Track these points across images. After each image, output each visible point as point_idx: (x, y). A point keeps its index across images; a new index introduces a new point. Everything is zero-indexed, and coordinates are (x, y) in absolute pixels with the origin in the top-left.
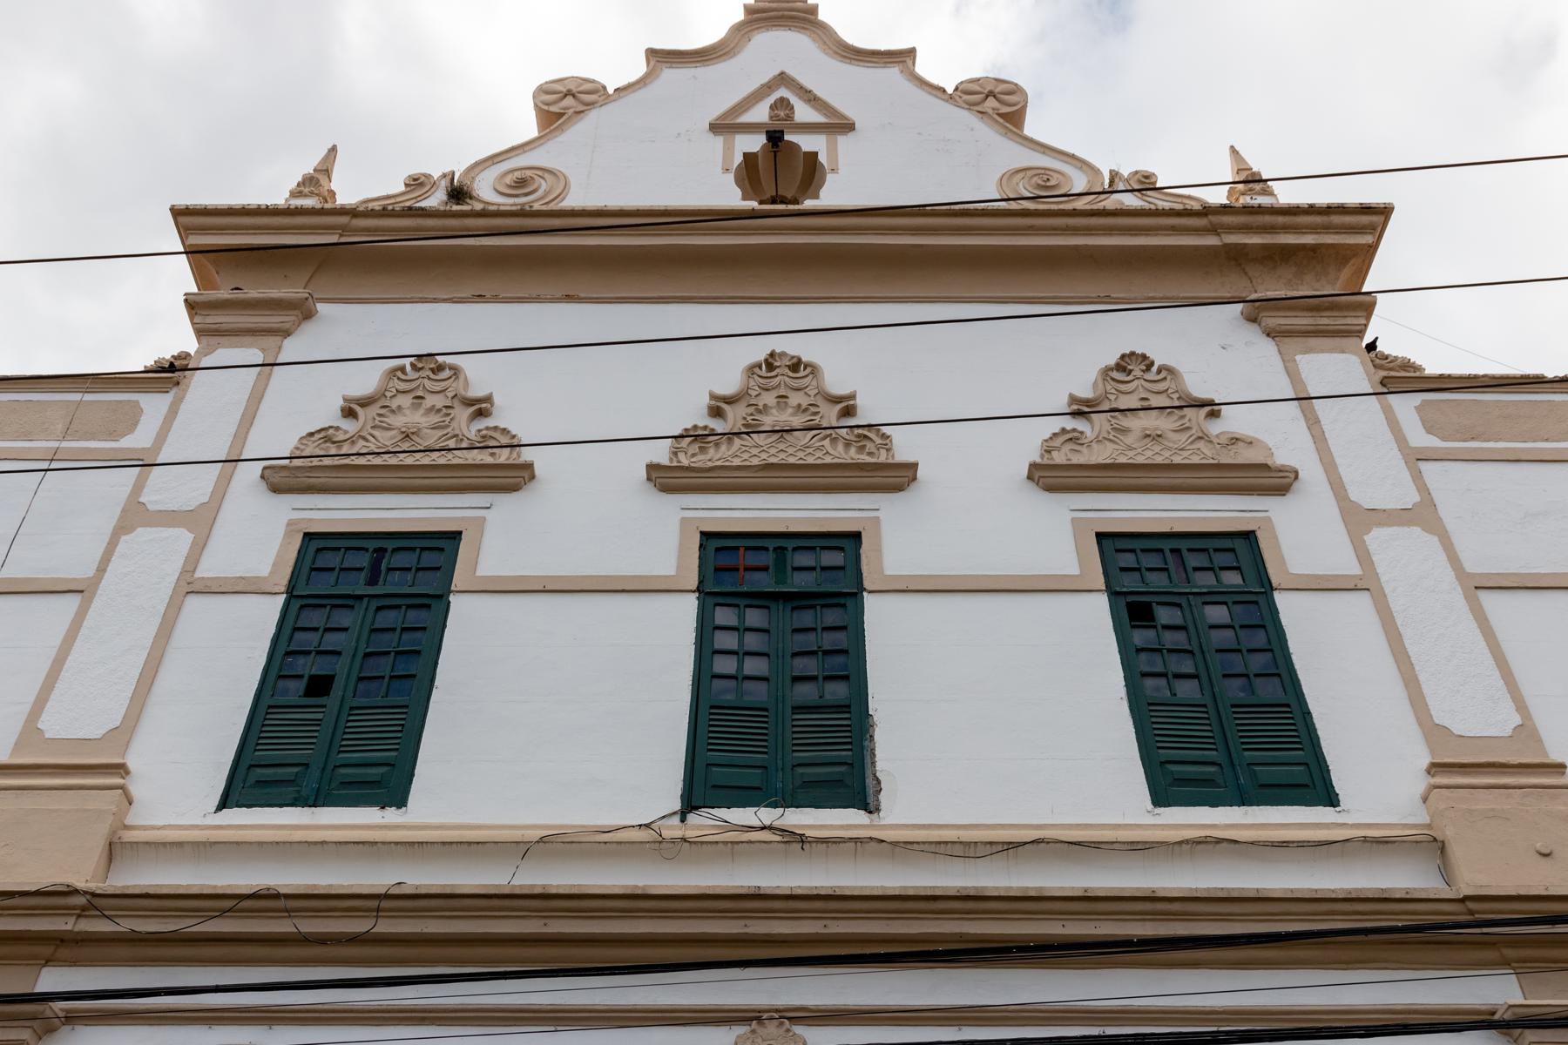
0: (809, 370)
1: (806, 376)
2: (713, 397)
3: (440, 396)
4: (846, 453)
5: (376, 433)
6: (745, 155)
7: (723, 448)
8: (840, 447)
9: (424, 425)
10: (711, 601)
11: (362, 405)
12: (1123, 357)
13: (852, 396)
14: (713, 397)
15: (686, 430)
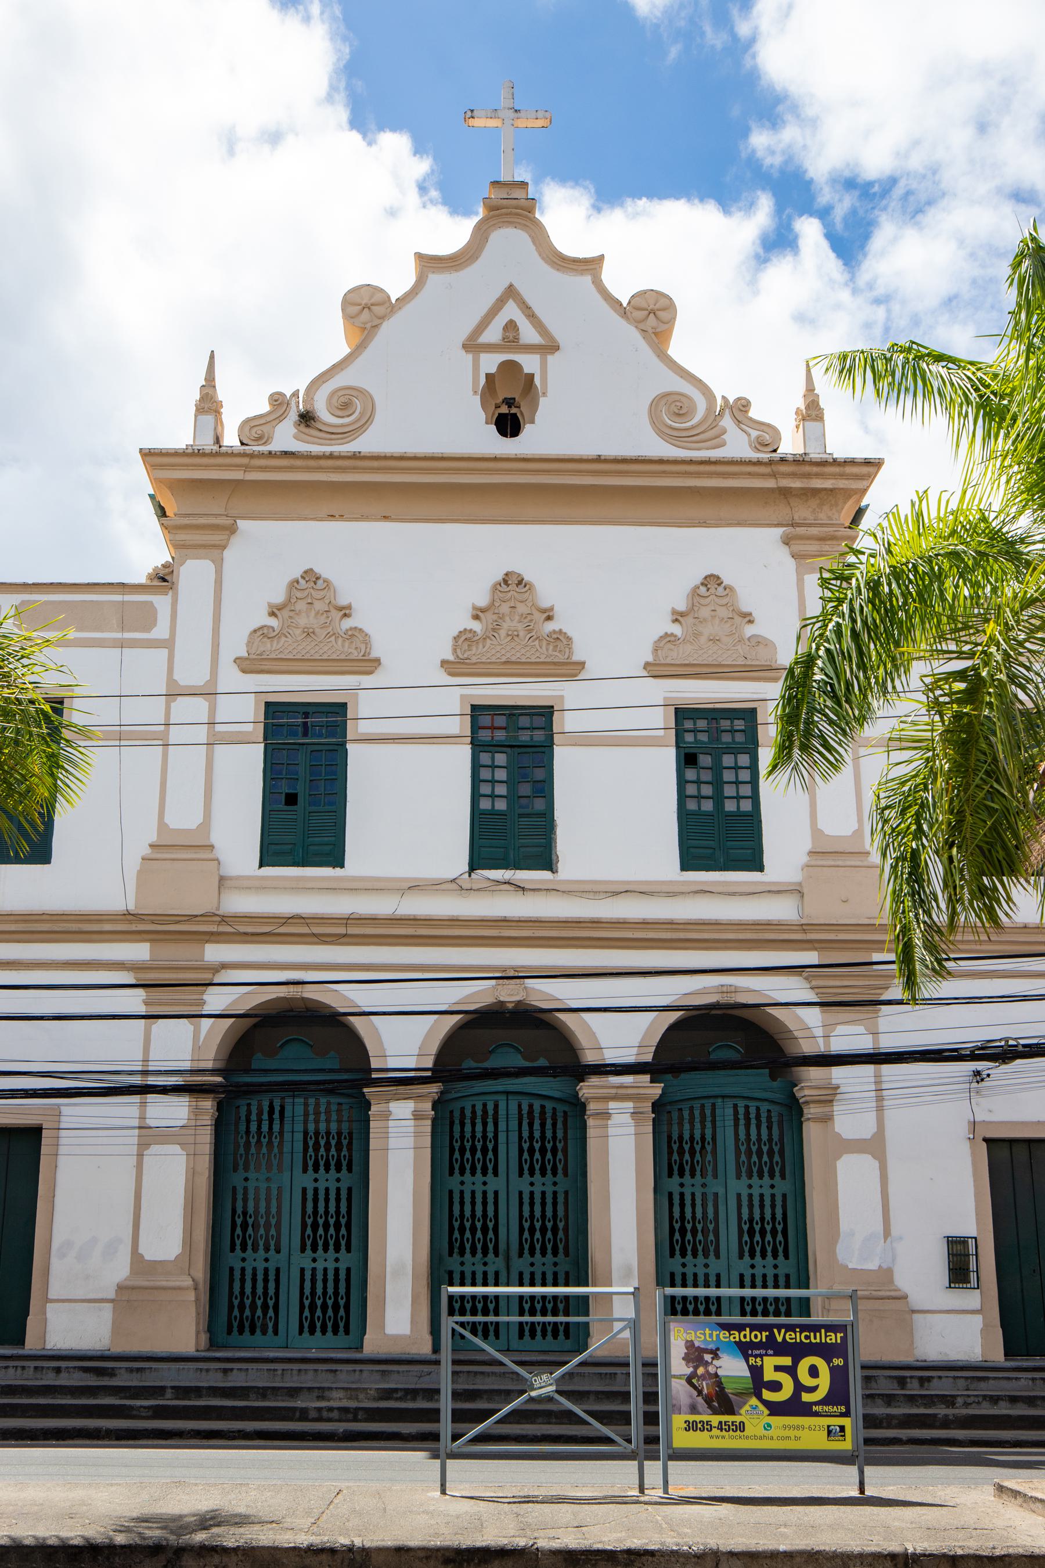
2: (475, 608)
7: (481, 646)
10: (478, 749)
11: (279, 610)
12: (706, 578)
13: (552, 609)
14: (475, 608)
15: (460, 632)
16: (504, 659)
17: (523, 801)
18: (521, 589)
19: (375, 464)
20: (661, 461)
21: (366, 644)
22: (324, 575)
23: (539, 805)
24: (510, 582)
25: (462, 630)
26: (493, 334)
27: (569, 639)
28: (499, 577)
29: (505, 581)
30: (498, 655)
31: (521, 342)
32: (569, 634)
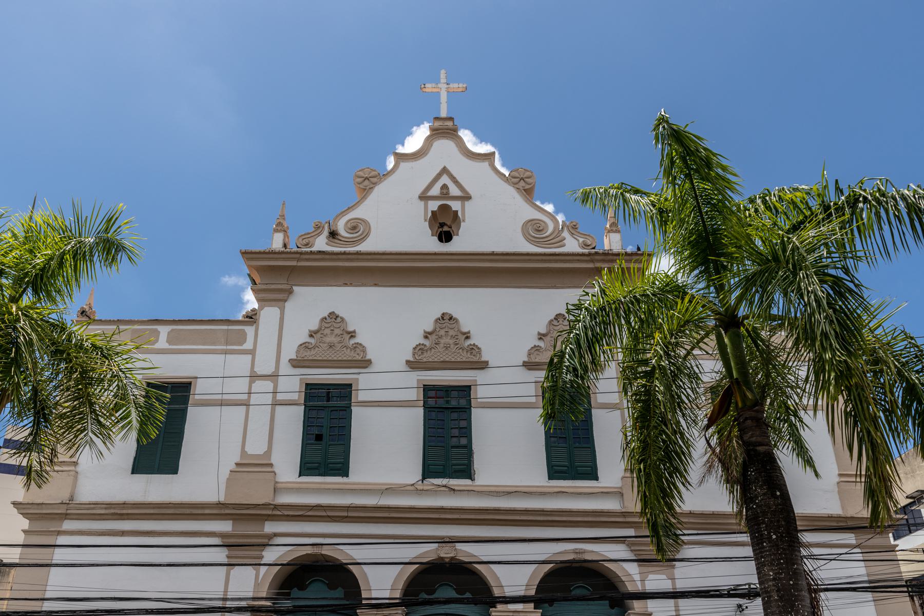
0: (455, 321)
1: (454, 323)
2: (425, 332)
3: (338, 329)
4: (467, 355)
5: (321, 345)
6: (432, 211)
7: (429, 352)
8: (465, 353)
9: (336, 342)
10: (427, 410)
11: (315, 333)
13: (469, 332)
14: (425, 332)
15: (417, 345)
16: (442, 360)
17: (455, 440)
18: (452, 322)
19: (369, 257)
20: (528, 254)
21: (364, 352)
22: (340, 315)
23: (464, 441)
24: (445, 318)
25: (418, 344)
26: (436, 191)
27: (479, 348)
28: (439, 316)
29: (443, 318)
30: (439, 357)
31: (451, 195)
32: (479, 346)
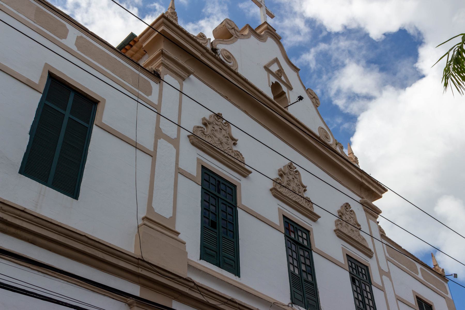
11: (209, 124)
